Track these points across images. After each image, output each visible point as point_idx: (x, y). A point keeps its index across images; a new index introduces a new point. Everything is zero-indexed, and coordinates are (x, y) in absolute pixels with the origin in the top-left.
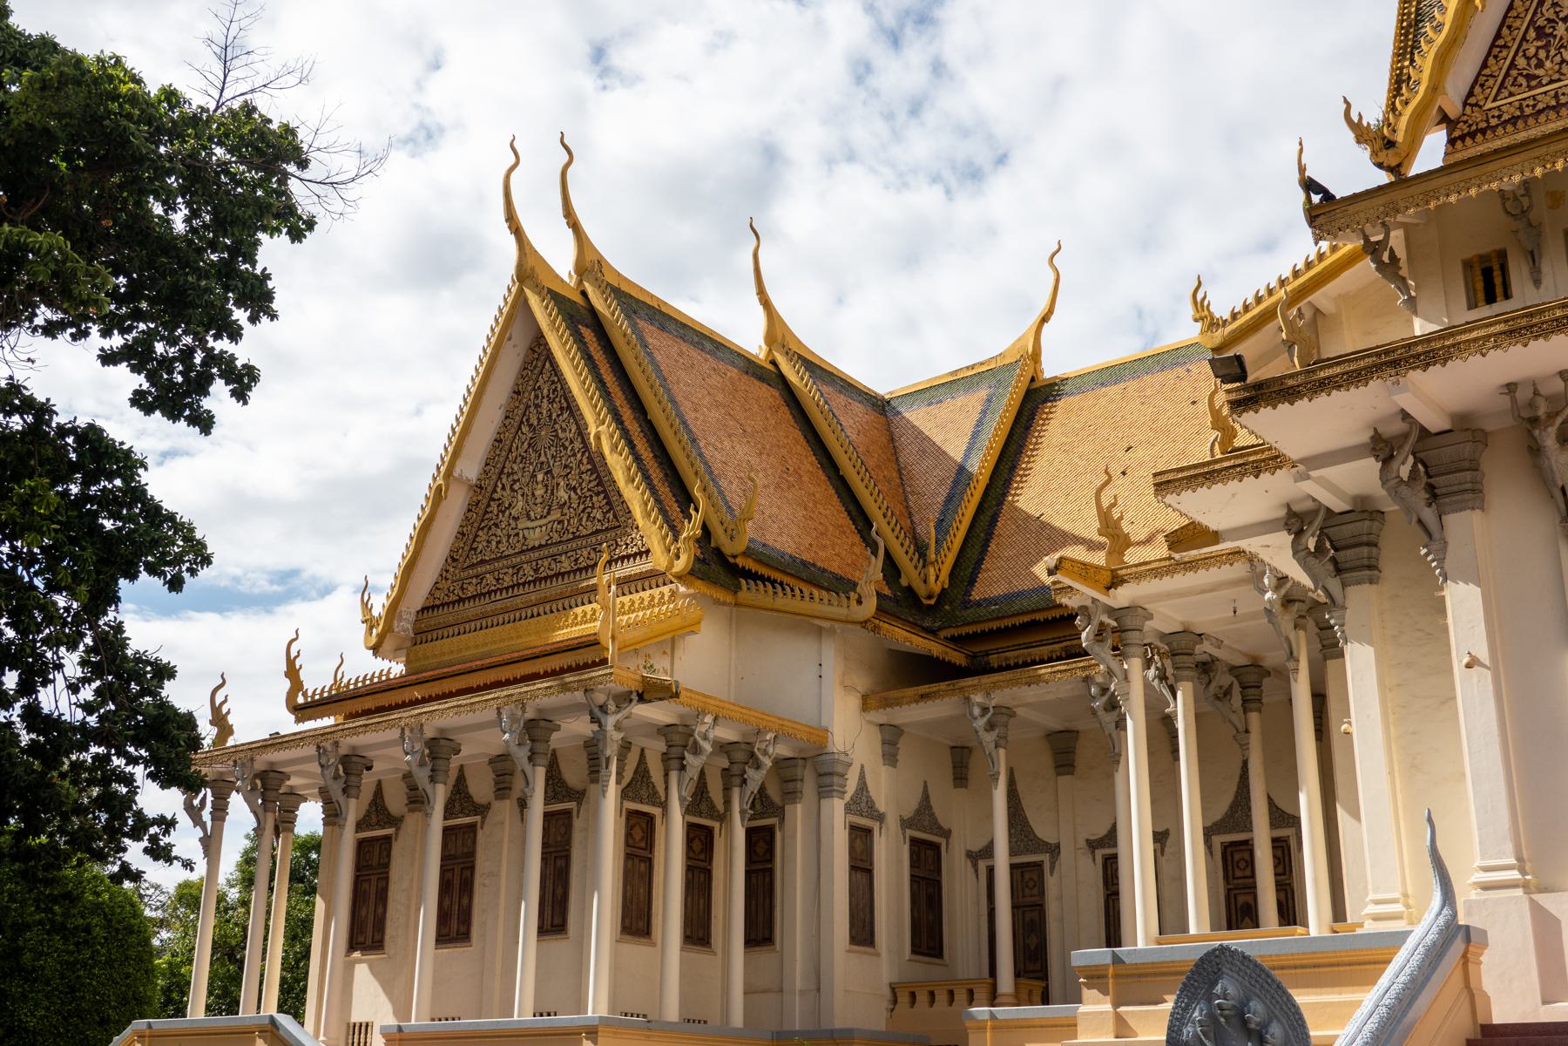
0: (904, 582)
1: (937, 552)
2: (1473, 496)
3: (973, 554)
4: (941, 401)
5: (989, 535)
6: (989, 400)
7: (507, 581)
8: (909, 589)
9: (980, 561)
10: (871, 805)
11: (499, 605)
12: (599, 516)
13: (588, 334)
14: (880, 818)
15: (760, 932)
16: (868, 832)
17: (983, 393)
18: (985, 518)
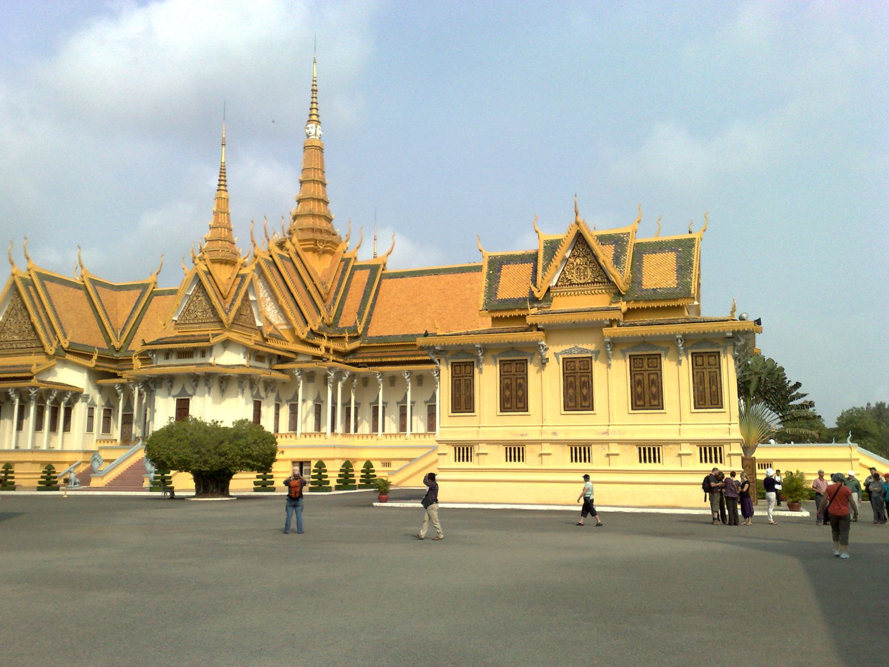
0: (112, 344)
1: (120, 339)
2: (161, 387)
3: (130, 337)
4: (130, 290)
5: (135, 333)
6: (141, 293)
7: (9, 347)
8: (113, 346)
9: (132, 340)
10: (94, 403)
11: (7, 352)
12: (33, 336)
13: (31, 288)
14: (96, 406)
15: (67, 428)
16: (93, 408)
17: (141, 291)
18: (135, 327)
